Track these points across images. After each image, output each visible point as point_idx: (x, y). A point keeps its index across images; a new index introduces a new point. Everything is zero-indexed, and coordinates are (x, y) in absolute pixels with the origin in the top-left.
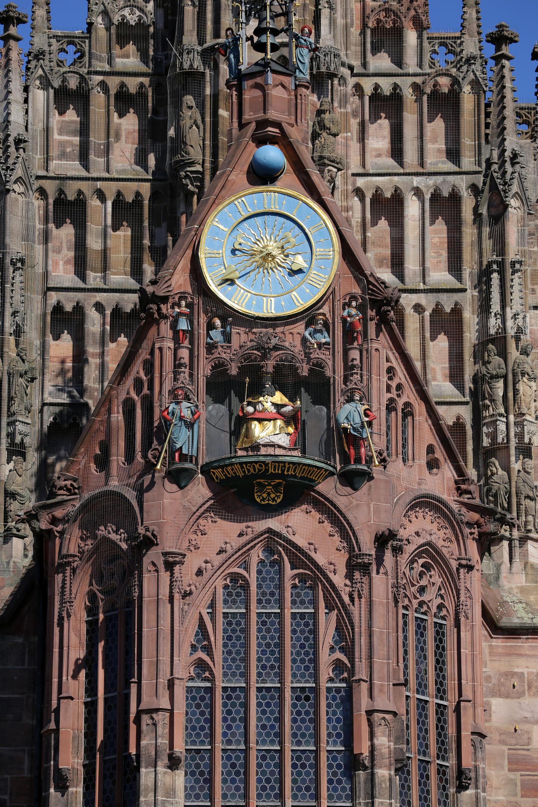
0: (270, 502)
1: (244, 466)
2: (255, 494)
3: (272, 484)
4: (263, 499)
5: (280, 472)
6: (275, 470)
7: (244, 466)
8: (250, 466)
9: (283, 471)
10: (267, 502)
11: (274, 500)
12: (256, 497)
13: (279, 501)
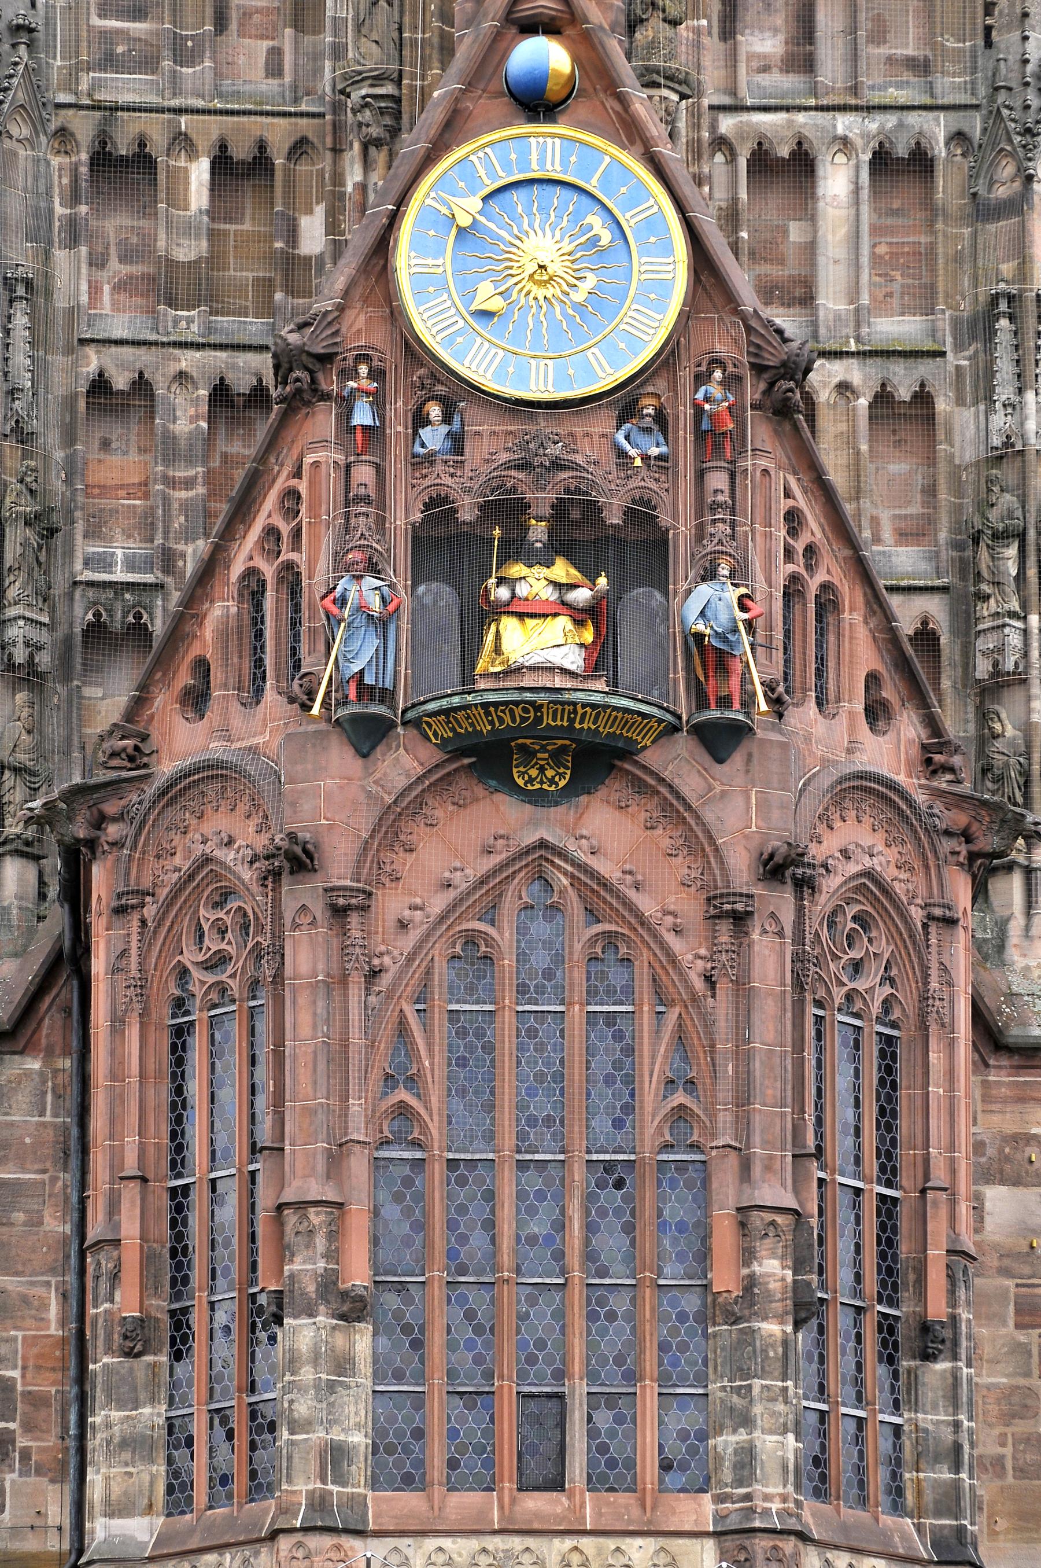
0: (545, 786)
2: (515, 770)
4: (531, 780)
5: (565, 724)
6: (554, 720)
7: (492, 709)
8: (503, 711)
9: (572, 721)
10: (538, 786)
11: (552, 781)
12: (516, 776)
13: (562, 783)
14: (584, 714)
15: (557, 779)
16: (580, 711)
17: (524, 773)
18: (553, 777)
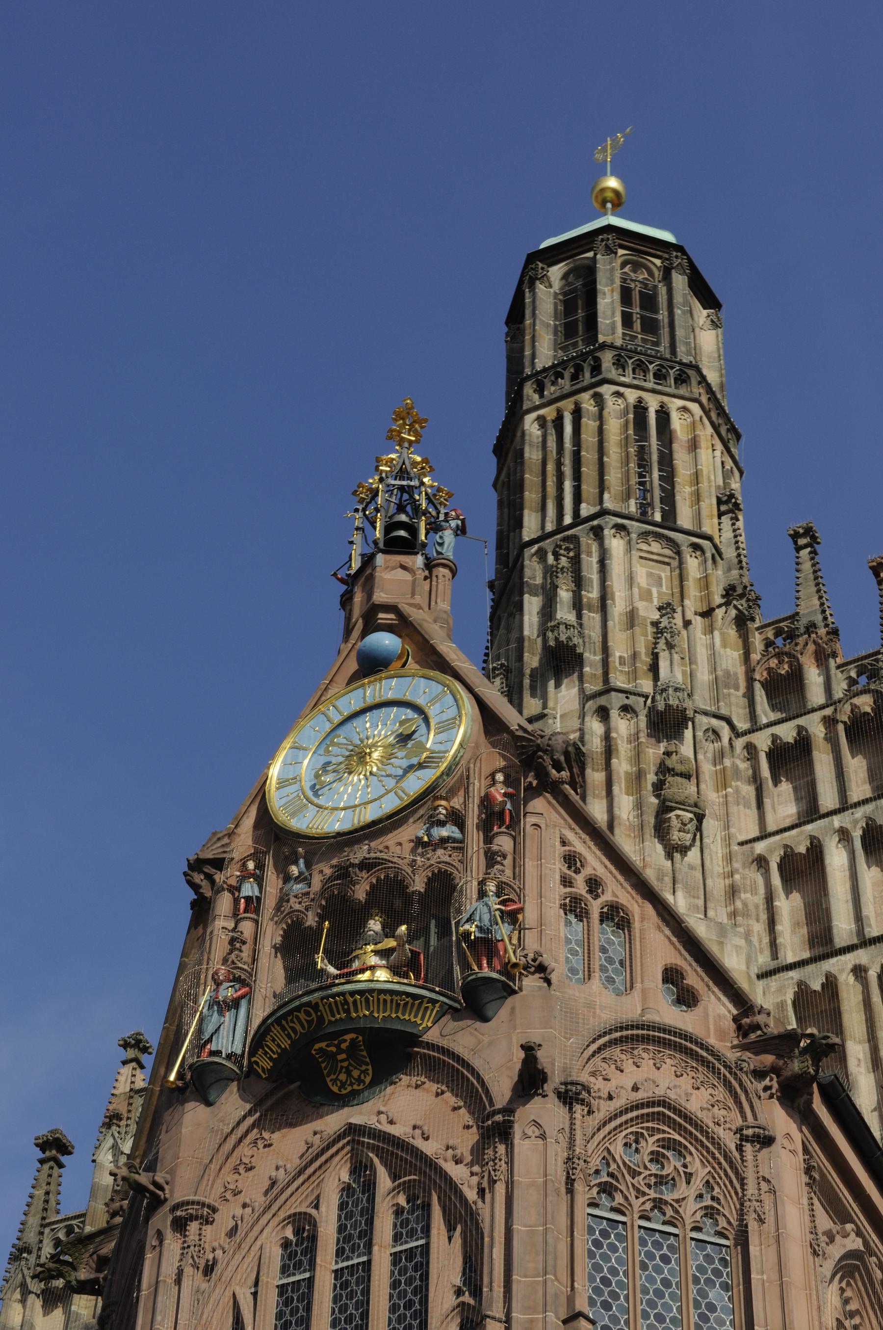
0: (355, 1087)
1: (284, 1022)
2: (328, 1080)
3: (344, 1046)
4: (343, 1085)
7: (284, 1022)
9: (347, 1011)
10: (349, 1089)
11: (360, 1081)
12: (330, 1084)
13: (368, 1080)
14: (355, 1002)
15: (362, 1077)
16: (350, 1000)
17: (337, 1079)
18: (359, 1076)
